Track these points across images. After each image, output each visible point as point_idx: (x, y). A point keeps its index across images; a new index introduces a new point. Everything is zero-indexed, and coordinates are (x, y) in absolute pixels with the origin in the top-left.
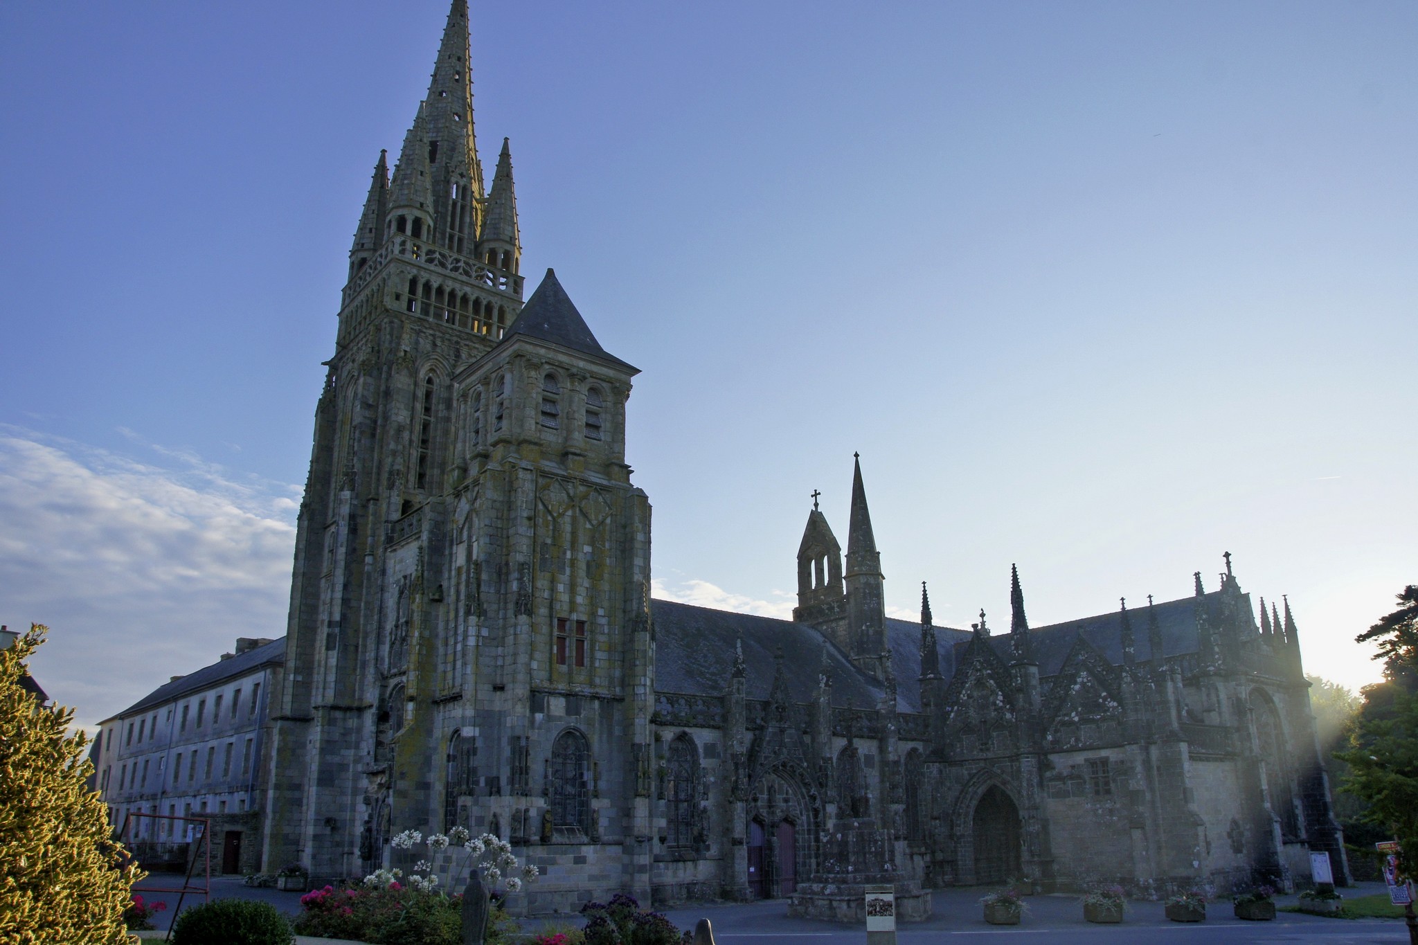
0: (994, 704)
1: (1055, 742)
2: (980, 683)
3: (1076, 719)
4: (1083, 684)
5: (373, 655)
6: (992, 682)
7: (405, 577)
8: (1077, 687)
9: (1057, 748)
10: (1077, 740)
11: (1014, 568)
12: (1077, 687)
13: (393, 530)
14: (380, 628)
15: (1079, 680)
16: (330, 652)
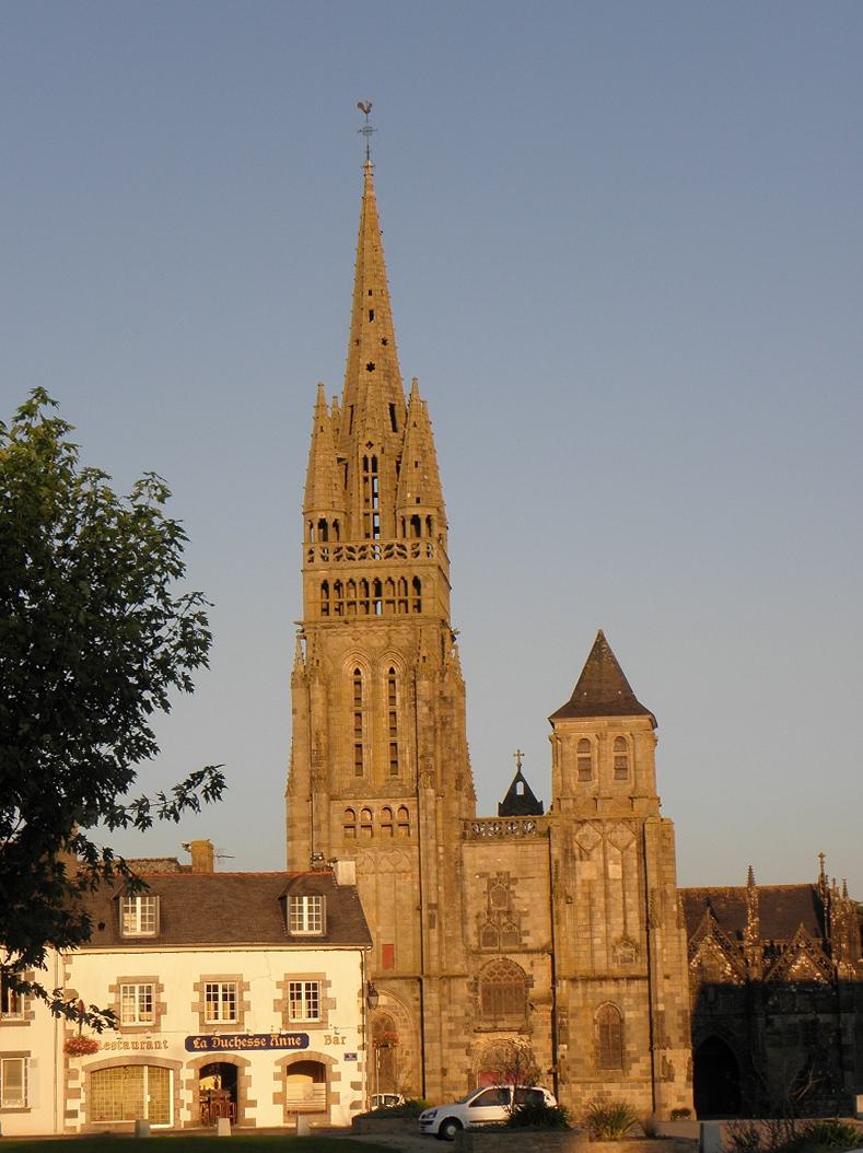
0: (723, 972)
1: (776, 1006)
2: (711, 955)
3: (795, 990)
4: (802, 965)
5: (459, 933)
6: (722, 955)
7: (498, 874)
8: (797, 967)
9: (776, 1009)
10: (794, 1006)
11: (750, 870)
12: (797, 967)
13: (466, 828)
14: (463, 911)
15: (799, 962)
16: (432, 930)
